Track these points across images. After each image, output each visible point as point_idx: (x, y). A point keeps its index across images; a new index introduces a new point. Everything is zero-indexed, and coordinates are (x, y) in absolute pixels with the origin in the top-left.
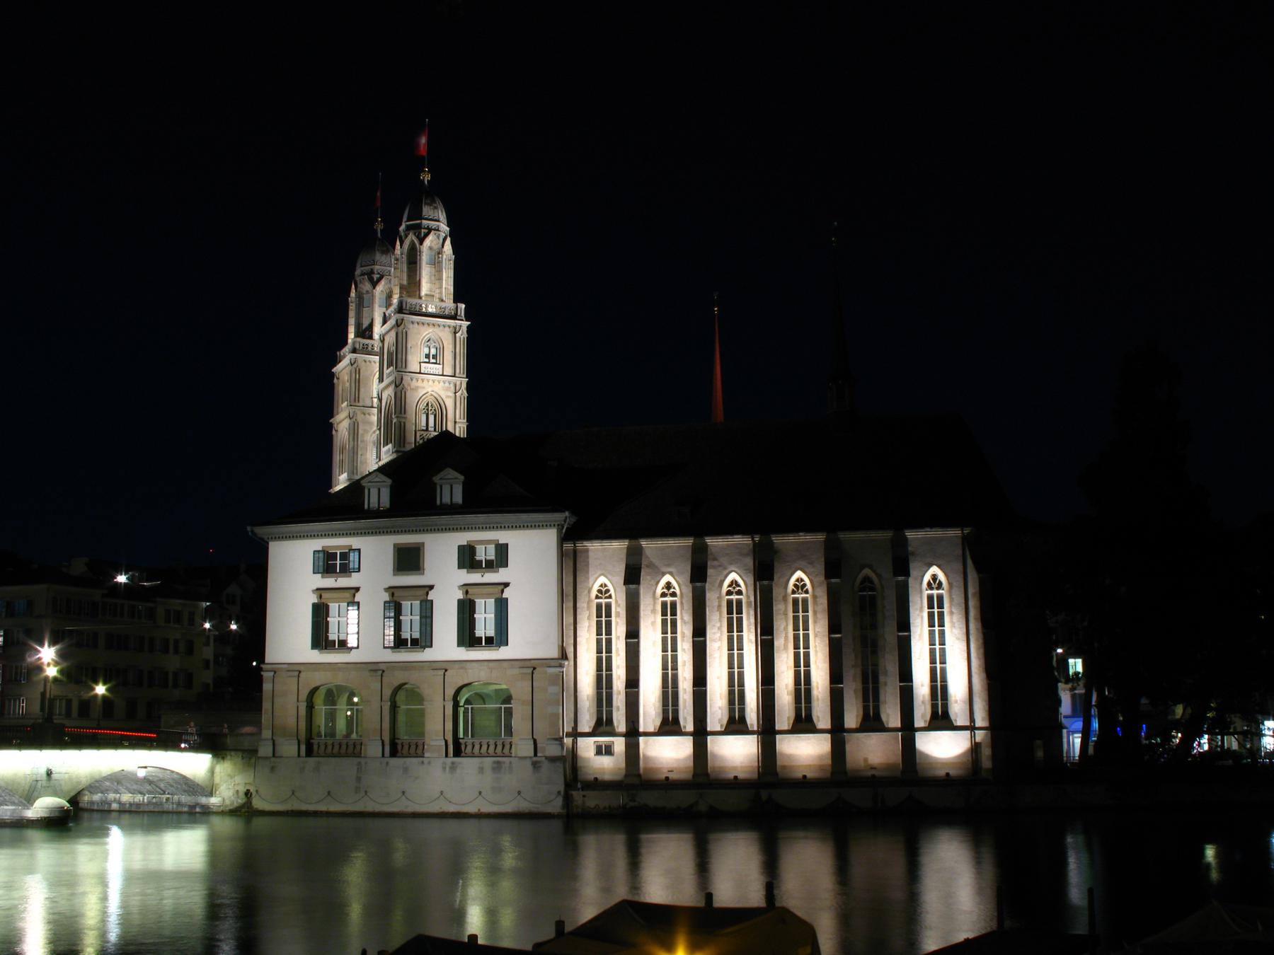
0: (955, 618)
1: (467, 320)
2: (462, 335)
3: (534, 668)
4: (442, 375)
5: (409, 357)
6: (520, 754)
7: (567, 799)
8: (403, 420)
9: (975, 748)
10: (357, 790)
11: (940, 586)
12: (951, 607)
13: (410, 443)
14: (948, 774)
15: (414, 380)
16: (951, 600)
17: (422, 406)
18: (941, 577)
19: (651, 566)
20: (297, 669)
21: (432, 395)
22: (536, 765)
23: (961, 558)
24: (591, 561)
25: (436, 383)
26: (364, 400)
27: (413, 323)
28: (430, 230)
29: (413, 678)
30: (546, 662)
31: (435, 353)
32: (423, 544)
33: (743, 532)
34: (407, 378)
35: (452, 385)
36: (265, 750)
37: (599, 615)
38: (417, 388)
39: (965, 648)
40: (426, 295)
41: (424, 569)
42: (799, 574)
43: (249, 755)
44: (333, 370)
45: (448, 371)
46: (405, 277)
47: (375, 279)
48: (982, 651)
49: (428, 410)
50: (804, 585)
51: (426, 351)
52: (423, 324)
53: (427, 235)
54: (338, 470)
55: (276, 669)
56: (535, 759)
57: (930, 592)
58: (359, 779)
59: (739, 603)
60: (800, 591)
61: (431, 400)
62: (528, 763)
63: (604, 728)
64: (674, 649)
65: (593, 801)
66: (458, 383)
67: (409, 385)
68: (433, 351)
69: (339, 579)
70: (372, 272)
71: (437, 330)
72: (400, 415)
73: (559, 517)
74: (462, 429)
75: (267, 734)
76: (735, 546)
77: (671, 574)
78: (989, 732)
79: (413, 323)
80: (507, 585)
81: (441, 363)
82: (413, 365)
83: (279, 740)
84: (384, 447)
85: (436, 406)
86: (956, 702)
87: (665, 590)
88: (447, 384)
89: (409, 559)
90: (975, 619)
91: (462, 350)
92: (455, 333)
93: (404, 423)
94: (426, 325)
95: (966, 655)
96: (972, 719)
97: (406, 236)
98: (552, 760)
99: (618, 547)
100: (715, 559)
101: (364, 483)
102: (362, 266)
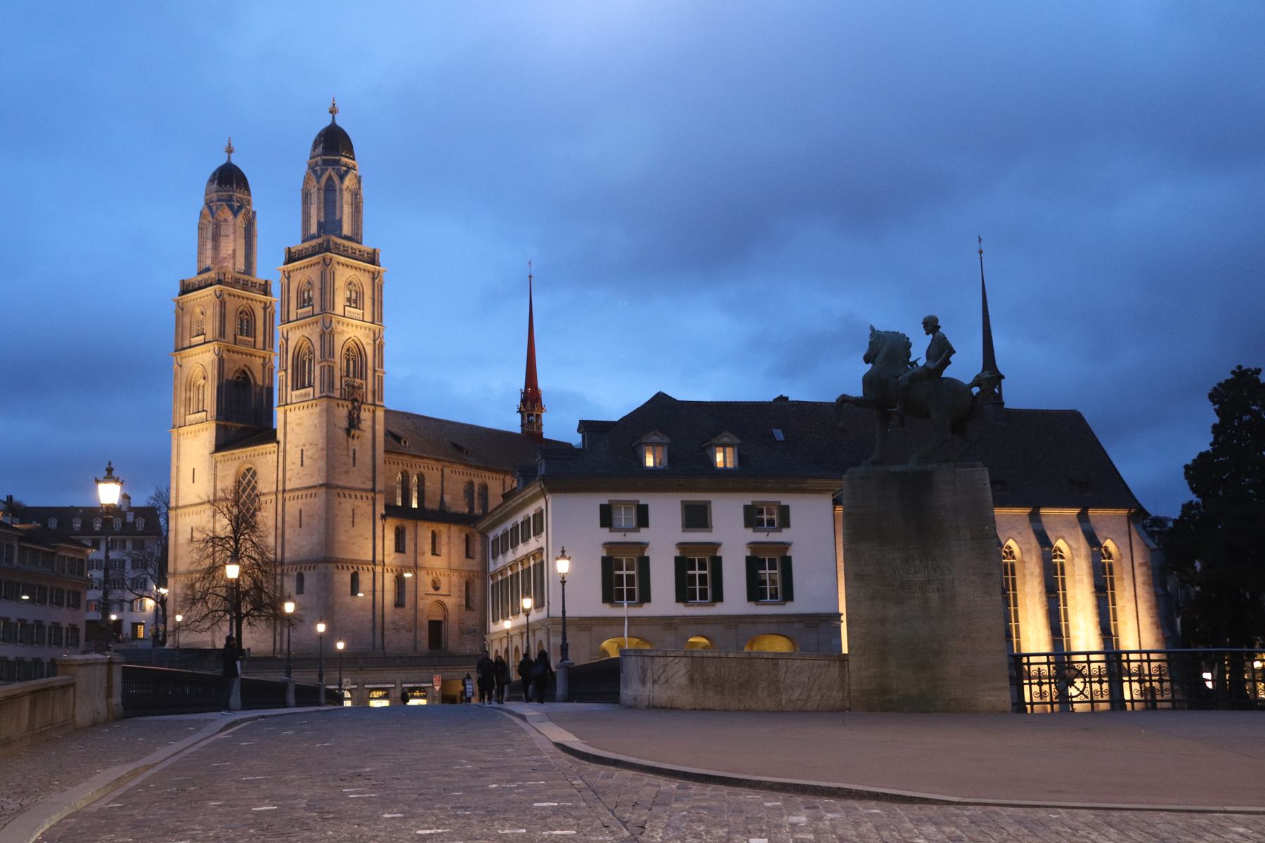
4: (363, 321)
8: (332, 364)
11: (1110, 556)
15: (340, 324)
21: (353, 340)
23: (1127, 534)
25: (359, 328)
27: (338, 263)
31: (354, 298)
32: (710, 502)
33: (1125, 508)
35: (372, 332)
38: (342, 332)
39: (1135, 608)
41: (712, 527)
45: (368, 317)
46: (322, 214)
50: (1011, 552)
53: (347, 172)
54: (183, 409)
60: (1009, 557)
61: (350, 344)
66: (377, 331)
67: (336, 328)
71: (358, 273)
79: (338, 263)
81: (361, 308)
82: (339, 309)
84: (292, 390)
88: (367, 331)
89: (696, 517)
93: (333, 367)
94: (354, 269)
97: (323, 171)
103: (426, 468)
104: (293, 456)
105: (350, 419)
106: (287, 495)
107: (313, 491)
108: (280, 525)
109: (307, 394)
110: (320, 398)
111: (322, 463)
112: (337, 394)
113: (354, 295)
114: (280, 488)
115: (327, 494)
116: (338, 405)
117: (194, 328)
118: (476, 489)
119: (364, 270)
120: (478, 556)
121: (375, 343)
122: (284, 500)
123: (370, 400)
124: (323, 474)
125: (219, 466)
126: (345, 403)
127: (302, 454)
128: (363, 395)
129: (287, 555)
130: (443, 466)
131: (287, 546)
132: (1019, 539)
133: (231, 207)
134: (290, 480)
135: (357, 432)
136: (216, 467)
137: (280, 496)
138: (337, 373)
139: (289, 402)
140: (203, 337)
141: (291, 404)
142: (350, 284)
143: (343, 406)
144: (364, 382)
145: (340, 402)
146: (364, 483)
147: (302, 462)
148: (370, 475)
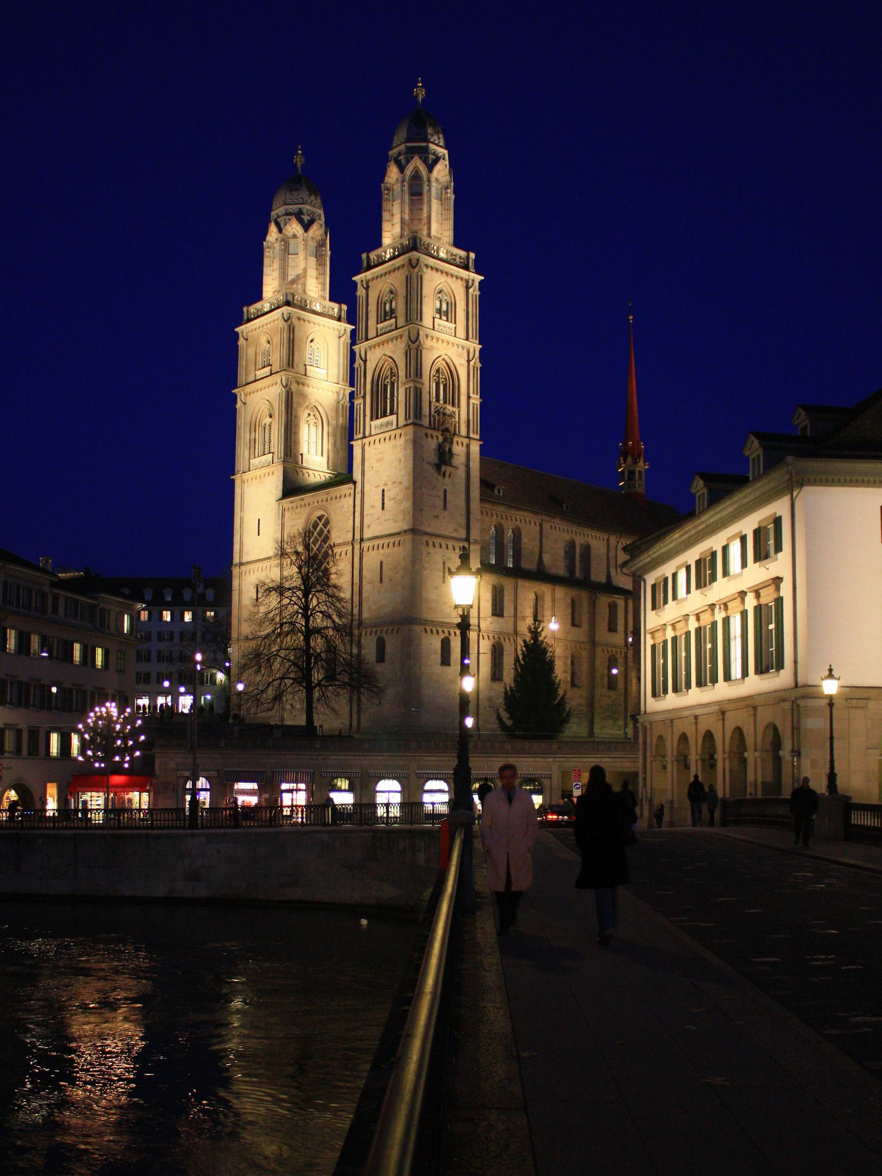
1: (477, 272)
2: (475, 291)
5: (424, 309)
8: (420, 386)
13: (425, 416)
15: (429, 338)
21: (444, 359)
25: (450, 345)
26: (297, 366)
38: (431, 349)
44: (237, 330)
45: (461, 333)
47: (306, 222)
49: (438, 377)
52: (437, 270)
54: (247, 452)
61: (440, 364)
66: (471, 350)
67: (424, 343)
71: (449, 280)
72: (417, 379)
74: (475, 407)
79: (427, 266)
82: (427, 321)
84: (372, 420)
88: (460, 349)
91: (474, 310)
92: (467, 288)
93: (421, 389)
94: (444, 274)
97: (408, 162)
102: (286, 204)
103: (523, 521)
104: (373, 497)
105: (440, 453)
106: (365, 545)
107: (397, 539)
108: (356, 580)
109: (389, 424)
110: (405, 426)
111: (408, 505)
112: (426, 421)
113: (444, 308)
114: (357, 536)
115: (414, 541)
116: (426, 435)
117: (260, 359)
118: (578, 550)
119: (457, 277)
120: (585, 626)
121: (469, 364)
122: (362, 551)
123: (463, 432)
124: (409, 518)
125: (287, 514)
126: (435, 433)
127: (383, 495)
128: (455, 425)
129: (365, 615)
130: (542, 520)
131: (364, 604)
133: (301, 221)
134: (368, 526)
135: (449, 469)
136: (283, 516)
137: (357, 546)
138: (425, 397)
139: (367, 435)
140: (269, 368)
141: (370, 436)
142: (440, 292)
143: (432, 437)
144: (456, 410)
145: (429, 432)
146: (456, 530)
147: (383, 504)
148: (463, 521)
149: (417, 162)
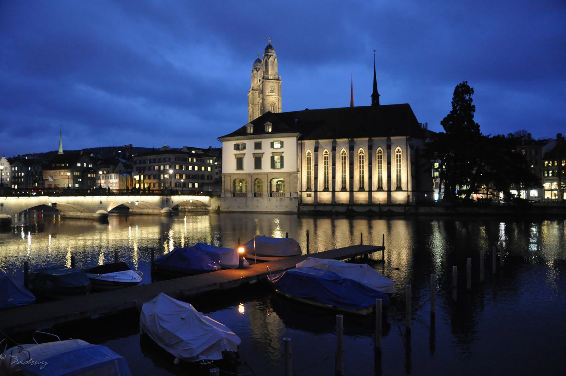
0: (404, 161)
3: (290, 174)
6: (287, 196)
7: (299, 208)
9: (408, 196)
10: (246, 205)
11: (400, 152)
12: (403, 158)
14: (400, 203)
16: (403, 156)
17: (270, 104)
18: (400, 150)
19: (322, 147)
20: (230, 175)
22: (291, 199)
23: (406, 145)
24: (306, 146)
28: (271, 56)
29: (259, 177)
30: (293, 173)
32: (261, 142)
34: (265, 97)
35: (278, 99)
36: (223, 196)
37: (308, 160)
38: (268, 100)
40: (270, 74)
42: (361, 149)
43: (219, 196)
45: (277, 95)
46: (264, 69)
48: (411, 170)
51: (270, 89)
53: (270, 57)
55: (225, 175)
56: (291, 198)
57: (397, 154)
58: (246, 203)
59: (345, 157)
61: (272, 103)
62: (289, 199)
63: (309, 190)
64: (328, 169)
65: (305, 209)
67: (266, 99)
68: (272, 89)
69: (241, 151)
70: (257, 68)
71: (273, 83)
73: (297, 134)
75: (223, 191)
76: (344, 141)
77: (327, 149)
78: (412, 192)
79: (267, 82)
80: (283, 152)
82: (267, 93)
83: (226, 193)
85: (273, 104)
86: (403, 184)
87: (325, 153)
88: (276, 98)
89: (258, 146)
90: (409, 161)
92: (278, 84)
95: (406, 171)
96: (408, 188)
97: (264, 58)
98: (295, 198)
99: (313, 142)
100: (339, 145)
101: (246, 126)
132: (364, 148)
133: (257, 70)
142: (271, 86)
149: (266, 58)
